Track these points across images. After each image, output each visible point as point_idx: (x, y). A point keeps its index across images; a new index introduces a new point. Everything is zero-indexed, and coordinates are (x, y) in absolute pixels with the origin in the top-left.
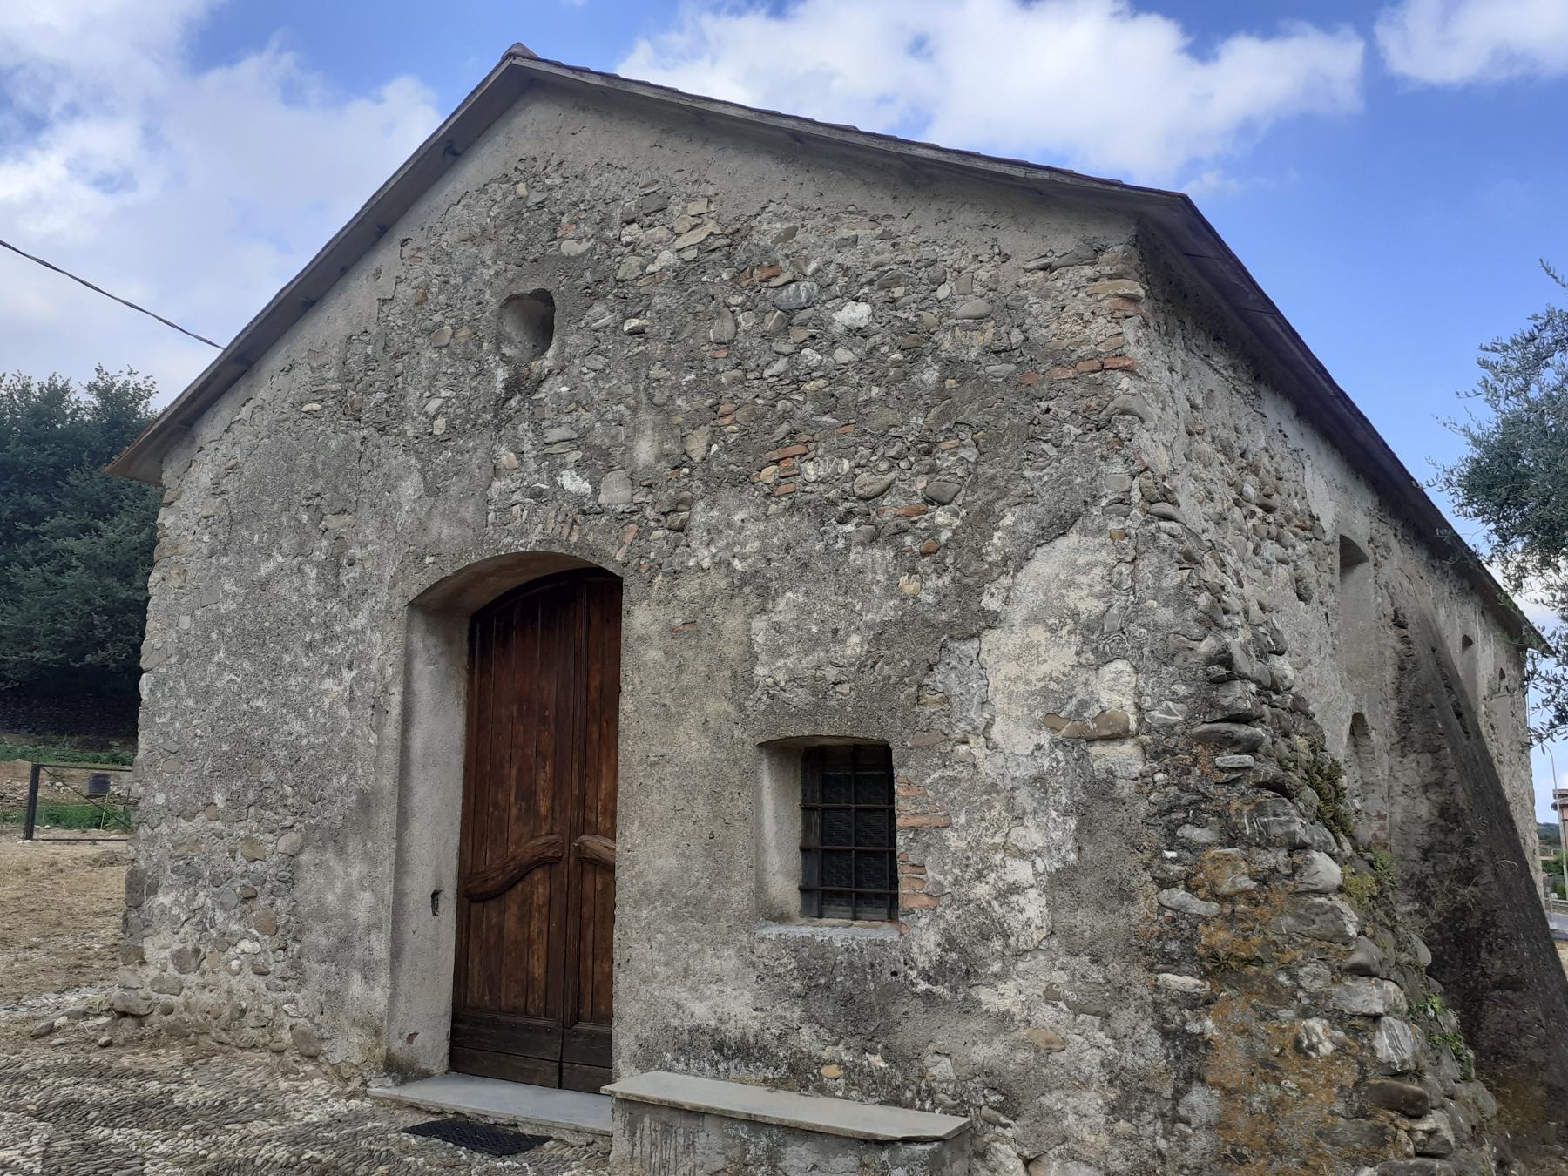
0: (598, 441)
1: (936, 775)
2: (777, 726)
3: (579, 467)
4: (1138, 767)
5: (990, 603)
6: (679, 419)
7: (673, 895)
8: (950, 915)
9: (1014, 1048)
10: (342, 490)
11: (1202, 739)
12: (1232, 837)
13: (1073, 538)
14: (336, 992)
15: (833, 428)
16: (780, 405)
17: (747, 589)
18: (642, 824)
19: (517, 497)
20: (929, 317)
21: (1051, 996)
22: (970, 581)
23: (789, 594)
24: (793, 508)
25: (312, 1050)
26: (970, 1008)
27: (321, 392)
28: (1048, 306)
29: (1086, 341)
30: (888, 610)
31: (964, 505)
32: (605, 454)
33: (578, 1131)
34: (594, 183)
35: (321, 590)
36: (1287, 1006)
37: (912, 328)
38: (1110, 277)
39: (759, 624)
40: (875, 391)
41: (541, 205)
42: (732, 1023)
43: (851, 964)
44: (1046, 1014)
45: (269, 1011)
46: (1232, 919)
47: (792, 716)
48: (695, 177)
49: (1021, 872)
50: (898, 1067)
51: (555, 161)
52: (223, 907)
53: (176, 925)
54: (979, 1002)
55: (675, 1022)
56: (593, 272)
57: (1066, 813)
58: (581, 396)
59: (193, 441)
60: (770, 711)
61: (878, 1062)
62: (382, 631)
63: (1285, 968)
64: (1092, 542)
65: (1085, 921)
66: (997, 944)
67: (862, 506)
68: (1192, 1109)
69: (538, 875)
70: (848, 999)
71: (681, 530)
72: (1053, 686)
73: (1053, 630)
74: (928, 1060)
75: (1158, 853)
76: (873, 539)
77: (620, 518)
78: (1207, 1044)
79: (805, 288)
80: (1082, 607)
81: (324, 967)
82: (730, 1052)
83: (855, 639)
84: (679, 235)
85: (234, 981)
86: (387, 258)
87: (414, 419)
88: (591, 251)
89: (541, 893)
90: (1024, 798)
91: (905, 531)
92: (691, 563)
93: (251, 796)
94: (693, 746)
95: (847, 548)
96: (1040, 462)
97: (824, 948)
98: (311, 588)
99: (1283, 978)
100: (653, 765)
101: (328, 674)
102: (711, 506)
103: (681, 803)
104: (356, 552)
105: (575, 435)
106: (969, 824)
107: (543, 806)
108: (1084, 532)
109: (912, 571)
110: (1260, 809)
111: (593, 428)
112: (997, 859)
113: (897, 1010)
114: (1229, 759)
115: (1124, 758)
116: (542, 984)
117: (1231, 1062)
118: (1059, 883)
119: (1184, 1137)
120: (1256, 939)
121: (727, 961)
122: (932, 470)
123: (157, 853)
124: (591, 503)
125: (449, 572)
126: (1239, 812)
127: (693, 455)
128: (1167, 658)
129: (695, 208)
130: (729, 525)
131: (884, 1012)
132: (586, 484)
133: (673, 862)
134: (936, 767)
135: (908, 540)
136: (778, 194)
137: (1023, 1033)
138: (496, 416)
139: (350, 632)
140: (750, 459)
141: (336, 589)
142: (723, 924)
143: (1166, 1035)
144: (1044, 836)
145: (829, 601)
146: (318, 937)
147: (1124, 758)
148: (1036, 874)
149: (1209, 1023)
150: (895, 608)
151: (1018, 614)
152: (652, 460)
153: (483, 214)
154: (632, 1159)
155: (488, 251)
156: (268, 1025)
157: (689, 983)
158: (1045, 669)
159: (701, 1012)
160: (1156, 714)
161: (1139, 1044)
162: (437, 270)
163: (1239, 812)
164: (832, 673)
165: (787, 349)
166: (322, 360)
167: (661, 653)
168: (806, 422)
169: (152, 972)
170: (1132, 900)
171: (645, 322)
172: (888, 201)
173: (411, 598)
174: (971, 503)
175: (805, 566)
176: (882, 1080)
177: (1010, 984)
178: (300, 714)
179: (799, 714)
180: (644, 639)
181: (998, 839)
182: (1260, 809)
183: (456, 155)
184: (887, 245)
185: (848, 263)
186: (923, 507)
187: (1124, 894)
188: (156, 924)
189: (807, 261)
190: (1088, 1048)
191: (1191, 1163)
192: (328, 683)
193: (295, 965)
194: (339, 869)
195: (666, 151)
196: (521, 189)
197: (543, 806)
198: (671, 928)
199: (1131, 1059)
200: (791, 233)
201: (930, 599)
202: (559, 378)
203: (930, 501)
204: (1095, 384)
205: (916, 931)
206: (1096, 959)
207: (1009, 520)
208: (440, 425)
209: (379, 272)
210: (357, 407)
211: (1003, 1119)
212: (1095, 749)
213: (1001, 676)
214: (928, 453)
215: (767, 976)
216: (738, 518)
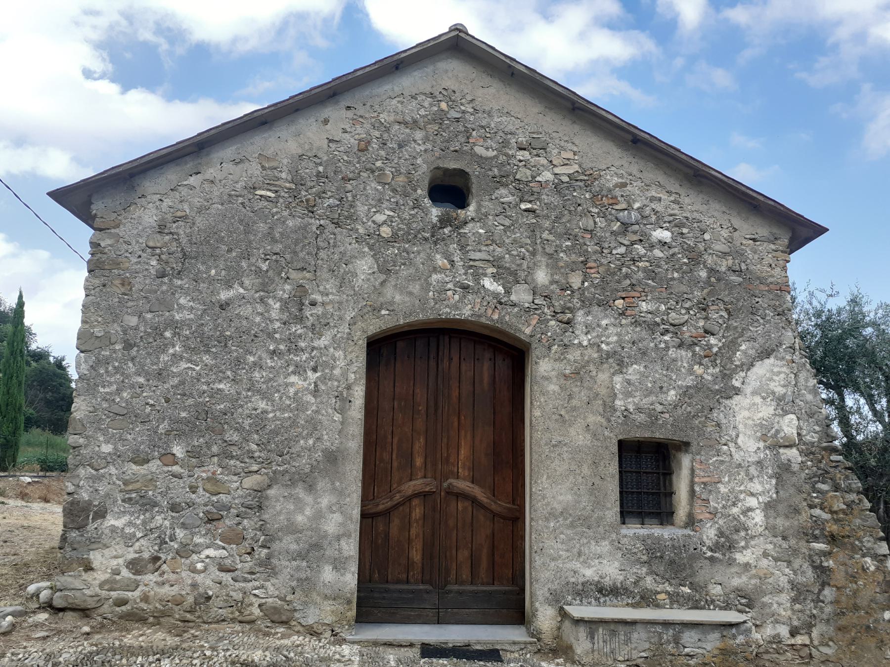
0: (508, 265)
1: (714, 459)
2: (630, 431)
3: (494, 276)
4: (800, 459)
5: (737, 384)
6: (561, 264)
7: (570, 515)
8: (721, 522)
9: (750, 578)
10: (301, 255)
11: (825, 449)
12: (837, 488)
13: (772, 360)
14: (307, 579)
15: (653, 287)
16: (624, 270)
17: (611, 360)
18: (548, 477)
19: (450, 286)
20: (701, 246)
21: (765, 555)
22: (727, 372)
23: (635, 366)
24: (636, 323)
25: (284, 618)
26: (731, 562)
27: (275, 186)
28: (756, 257)
29: (772, 276)
30: (689, 381)
31: (723, 337)
32: (514, 274)
33: (514, 643)
34: (496, 119)
35: (285, 317)
36: (857, 554)
37: (691, 249)
38: (782, 252)
39: (618, 379)
40: (676, 275)
41: (457, 120)
42: (608, 578)
43: (673, 546)
44: (764, 563)
45: (238, 596)
46: (837, 521)
47: (638, 427)
48: (566, 139)
49: (752, 502)
50: (697, 591)
51: (469, 98)
52: (184, 526)
53: (129, 540)
54: (735, 559)
55: (573, 580)
56: (499, 170)
57: (771, 477)
58: (496, 238)
59: (133, 188)
60: (625, 423)
61: (687, 590)
62: (345, 351)
63: (858, 539)
64: (779, 363)
65: (781, 523)
66: (743, 534)
67: (672, 329)
68: (825, 596)
69: (415, 502)
70: (672, 562)
71: (567, 323)
72: (764, 422)
73: (764, 398)
74: (710, 587)
75: (809, 494)
76: (680, 346)
77: (528, 310)
78: (830, 570)
79: (634, 215)
80: (776, 390)
81: (294, 563)
82: (606, 592)
83: (672, 392)
84: (555, 166)
85: (199, 578)
86: (337, 116)
87: (364, 223)
88: (496, 157)
89: (417, 513)
90: (753, 470)
91: (696, 344)
92: (576, 342)
93: (215, 449)
94: (579, 437)
95: (667, 348)
96: (756, 324)
97: (659, 539)
98: (274, 314)
99: (857, 543)
100: (554, 446)
101: (294, 373)
102: (588, 313)
103: (573, 467)
104: (318, 298)
105: (492, 259)
106: (729, 481)
107: (419, 461)
108: (776, 358)
109: (700, 364)
110: (847, 477)
111: (504, 258)
112: (742, 496)
113: (697, 565)
114: (834, 457)
115: (793, 455)
116: (420, 565)
117: (839, 577)
118: (768, 507)
119: (822, 608)
120: (847, 528)
121: (605, 546)
122: (707, 318)
123: (103, 488)
124: (506, 299)
125: (402, 322)
126: (840, 478)
127: (573, 285)
128: (811, 415)
129: (564, 155)
130: (599, 326)
131: (691, 567)
132: (501, 288)
133: (569, 497)
134: (714, 456)
135: (697, 349)
136: (617, 163)
137: (754, 571)
138: (433, 236)
139: (313, 349)
140: (608, 294)
141: (300, 319)
142: (601, 529)
143: (815, 568)
144: (762, 487)
145: (658, 372)
146: (289, 543)
147: (793, 455)
148: (759, 503)
149: (831, 562)
150: (692, 380)
151: (748, 389)
152: (547, 283)
153: (411, 110)
154: (593, 651)
155: (419, 135)
156: (241, 605)
157: (581, 560)
158: (761, 415)
159: (589, 573)
160: (808, 437)
161: (803, 572)
162: (377, 134)
163: (840, 478)
164: (659, 408)
165: (626, 243)
166: (274, 164)
167: (557, 387)
168: (640, 282)
169: (101, 576)
170: (800, 513)
171: (535, 207)
172: (677, 186)
173: (370, 333)
174: (728, 337)
175: (644, 354)
176: (689, 598)
177: (749, 551)
178: (265, 396)
179: (640, 426)
180: (547, 379)
181: (742, 488)
182: (847, 477)
183: (397, 68)
184: (676, 206)
185: (657, 209)
186: (704, 334)
187: (797, 511)
188: (106, 541)
189: (634, 201)
190: (782, 576)
191: (825, 617)
192: (293, 379)
193: (266, 563)
194: (309, 499)
195: (548, 118)
196: (444, 105)
197: (419, 461)
198: (569, 532)
199: (800, 579)
200: (624, 185)
201: (709, 378)
202: (478, 224)
203: (706, 332)
204: (777, 295)
205: (705, 529)
206: (784, 538)
207: (743, 347)
208: (386, 231)
209: (326, 122)
210: (312, 203)
211: (747, 610)
212: (782, 451)
213: (741, 416)
214: (704, 310)
215: (628, 554)
216: (604, 322)
